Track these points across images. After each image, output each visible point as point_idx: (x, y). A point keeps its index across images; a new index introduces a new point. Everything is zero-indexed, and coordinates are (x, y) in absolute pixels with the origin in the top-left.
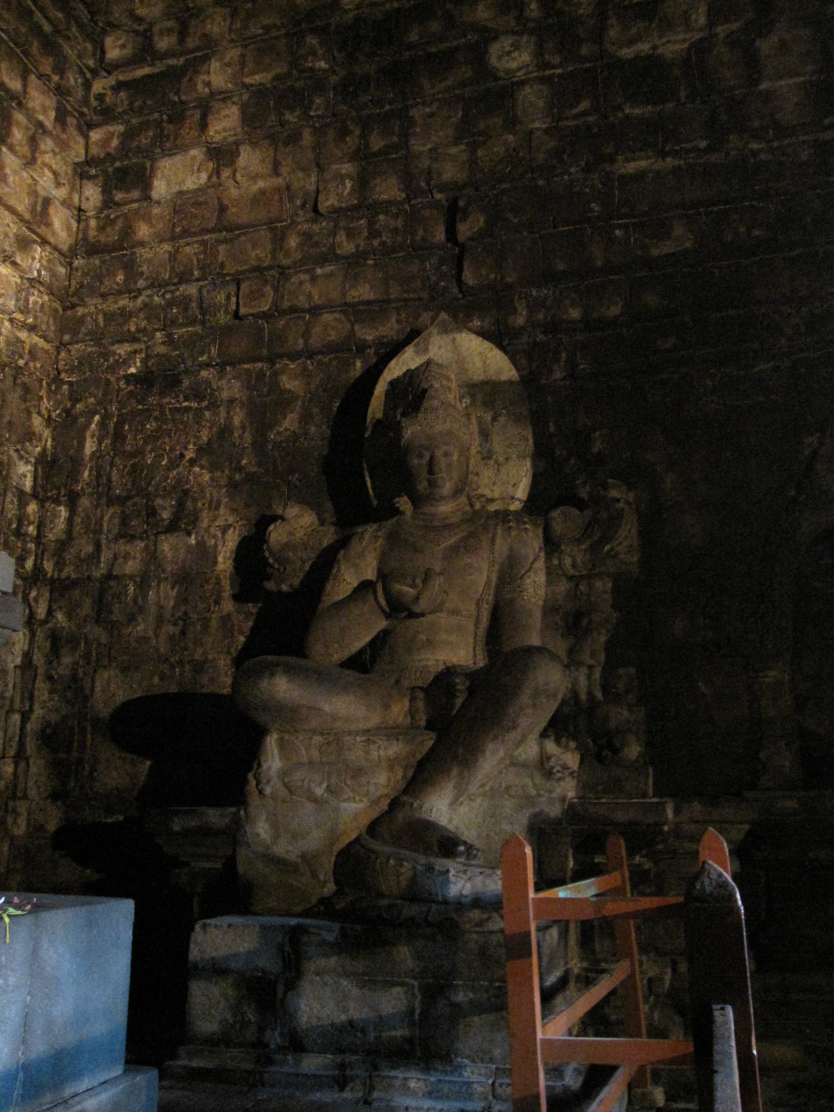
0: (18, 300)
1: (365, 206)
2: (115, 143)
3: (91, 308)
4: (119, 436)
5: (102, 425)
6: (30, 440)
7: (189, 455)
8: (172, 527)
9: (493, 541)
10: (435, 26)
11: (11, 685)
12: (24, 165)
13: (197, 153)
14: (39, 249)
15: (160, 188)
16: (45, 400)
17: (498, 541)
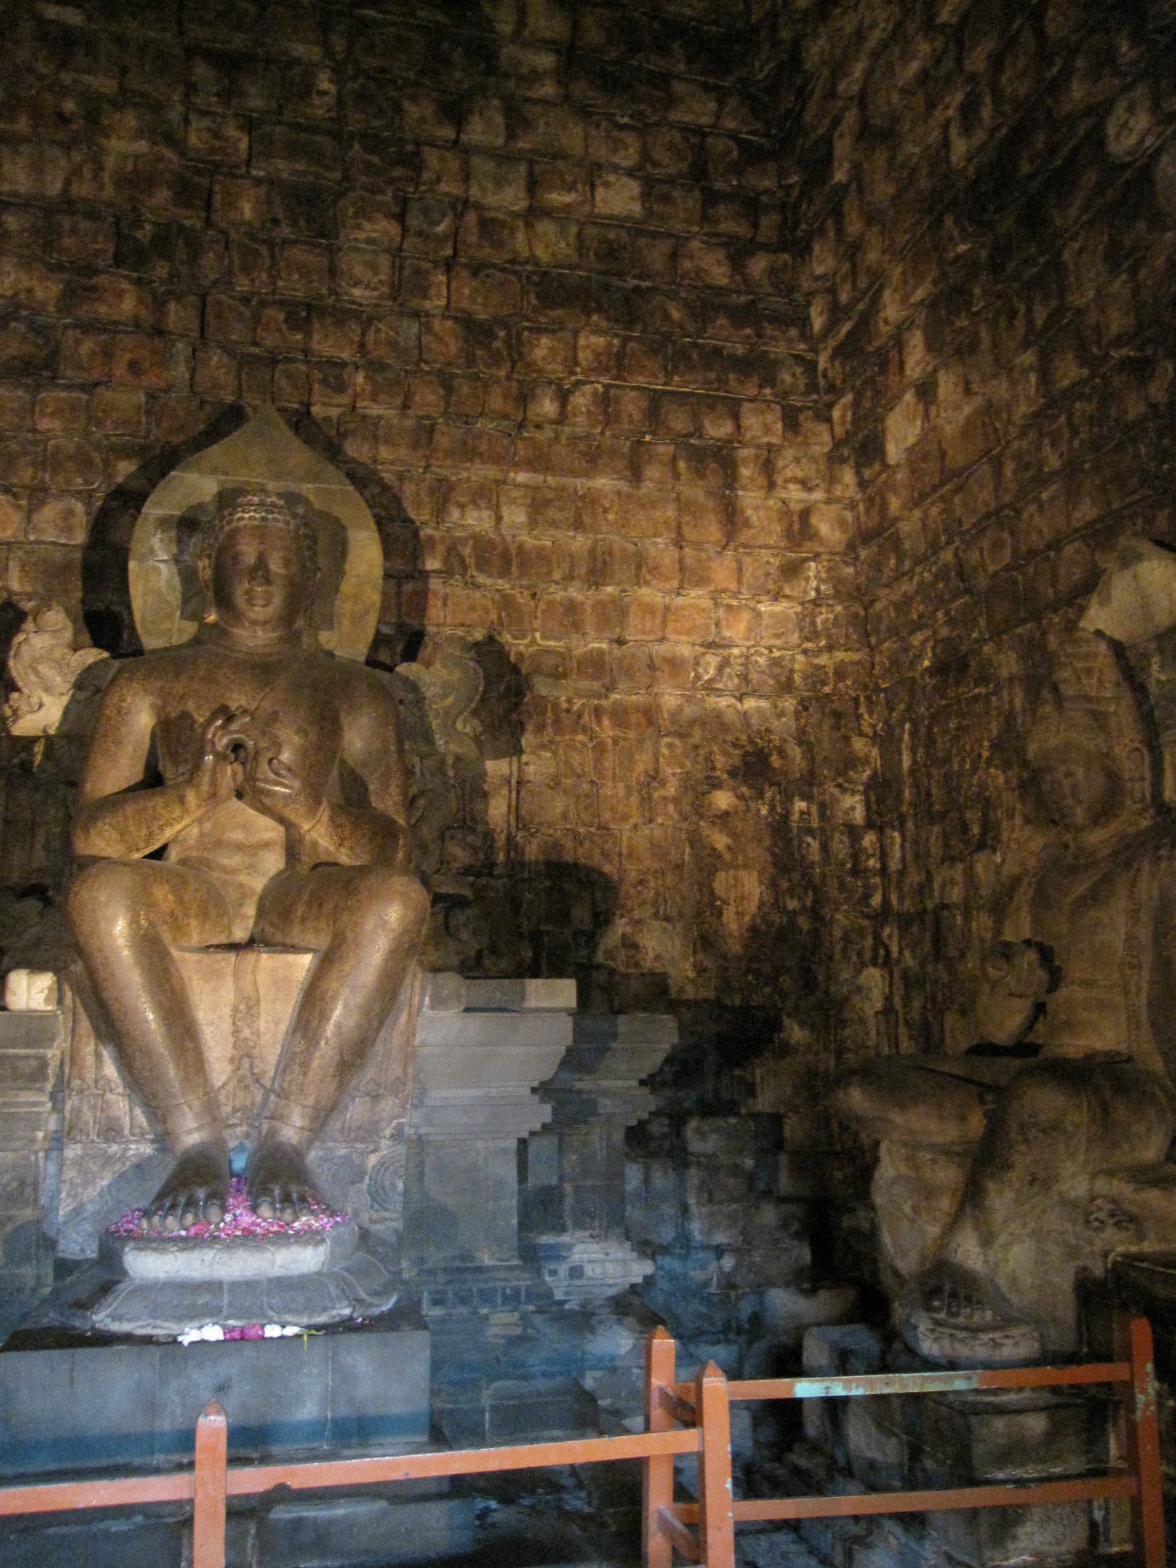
0: (801, 630)
1: (1054, 401)
2: (849, 418)
3: (884, 600)
4: (931, 741)
5: (914, 733)
6: (853, 767)
7: (985, 754)
8: (981, 846)
9: (1133, 884)
10: (1040, 140)
11: (873, 1033)
12: (220, 916)
13: (909, 397)
14: (813, 564)
15: (894, 452)
16: (866, 716)
17: (1144, 877)
